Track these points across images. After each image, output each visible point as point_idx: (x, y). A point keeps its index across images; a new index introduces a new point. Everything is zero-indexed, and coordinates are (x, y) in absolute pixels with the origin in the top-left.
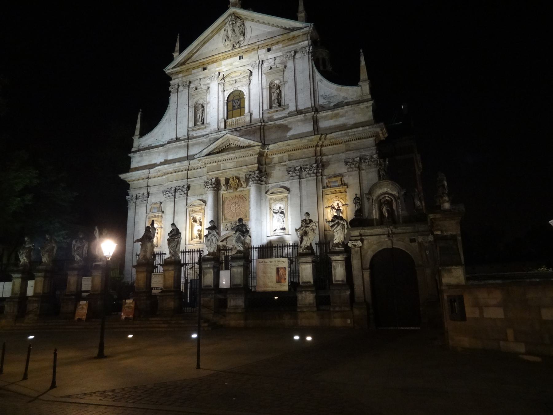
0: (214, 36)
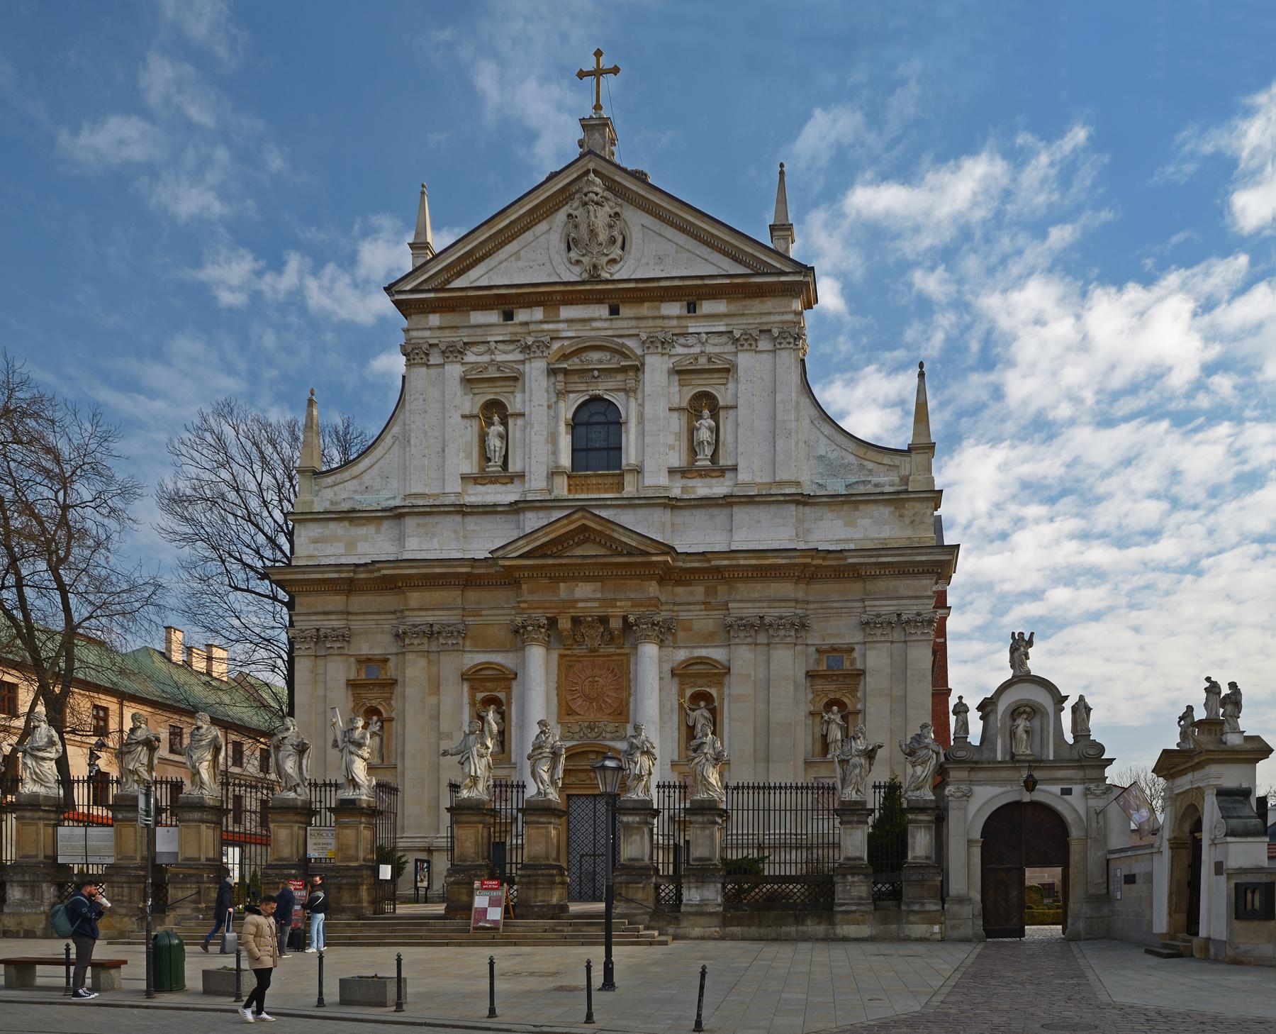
0: (536, 224)
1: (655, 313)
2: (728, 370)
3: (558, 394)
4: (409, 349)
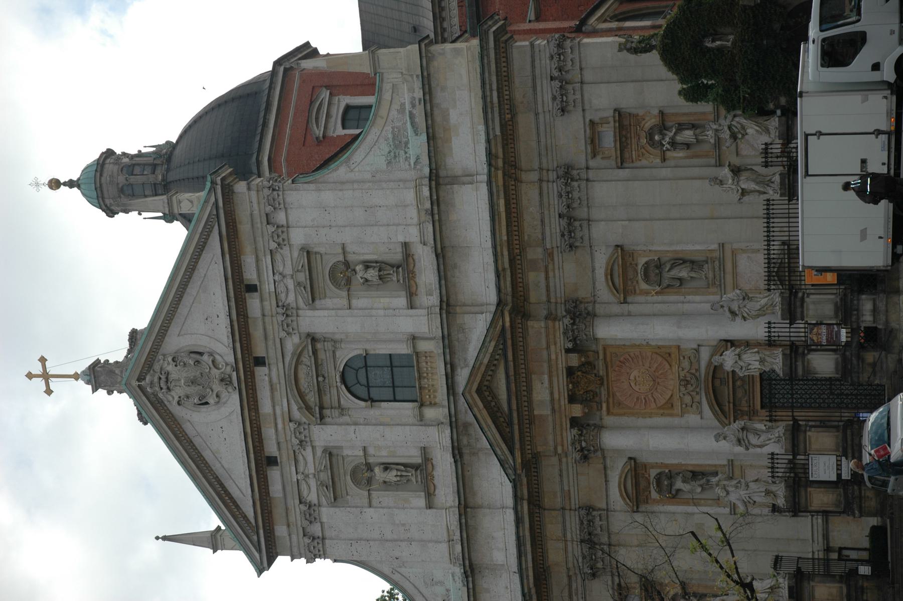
0: (186, 434)
1: (260, 323)
2: (308, 252)
3: (343, 415)
4: (309, 555)
